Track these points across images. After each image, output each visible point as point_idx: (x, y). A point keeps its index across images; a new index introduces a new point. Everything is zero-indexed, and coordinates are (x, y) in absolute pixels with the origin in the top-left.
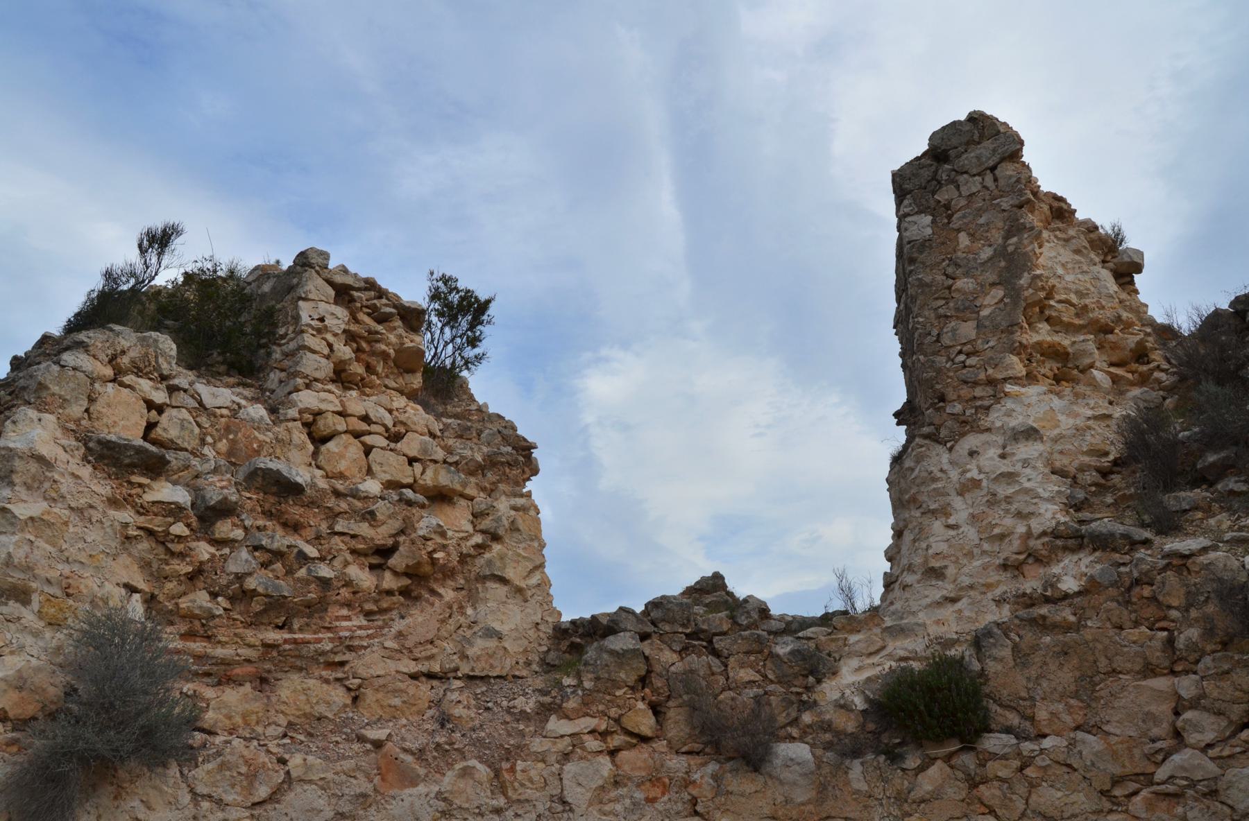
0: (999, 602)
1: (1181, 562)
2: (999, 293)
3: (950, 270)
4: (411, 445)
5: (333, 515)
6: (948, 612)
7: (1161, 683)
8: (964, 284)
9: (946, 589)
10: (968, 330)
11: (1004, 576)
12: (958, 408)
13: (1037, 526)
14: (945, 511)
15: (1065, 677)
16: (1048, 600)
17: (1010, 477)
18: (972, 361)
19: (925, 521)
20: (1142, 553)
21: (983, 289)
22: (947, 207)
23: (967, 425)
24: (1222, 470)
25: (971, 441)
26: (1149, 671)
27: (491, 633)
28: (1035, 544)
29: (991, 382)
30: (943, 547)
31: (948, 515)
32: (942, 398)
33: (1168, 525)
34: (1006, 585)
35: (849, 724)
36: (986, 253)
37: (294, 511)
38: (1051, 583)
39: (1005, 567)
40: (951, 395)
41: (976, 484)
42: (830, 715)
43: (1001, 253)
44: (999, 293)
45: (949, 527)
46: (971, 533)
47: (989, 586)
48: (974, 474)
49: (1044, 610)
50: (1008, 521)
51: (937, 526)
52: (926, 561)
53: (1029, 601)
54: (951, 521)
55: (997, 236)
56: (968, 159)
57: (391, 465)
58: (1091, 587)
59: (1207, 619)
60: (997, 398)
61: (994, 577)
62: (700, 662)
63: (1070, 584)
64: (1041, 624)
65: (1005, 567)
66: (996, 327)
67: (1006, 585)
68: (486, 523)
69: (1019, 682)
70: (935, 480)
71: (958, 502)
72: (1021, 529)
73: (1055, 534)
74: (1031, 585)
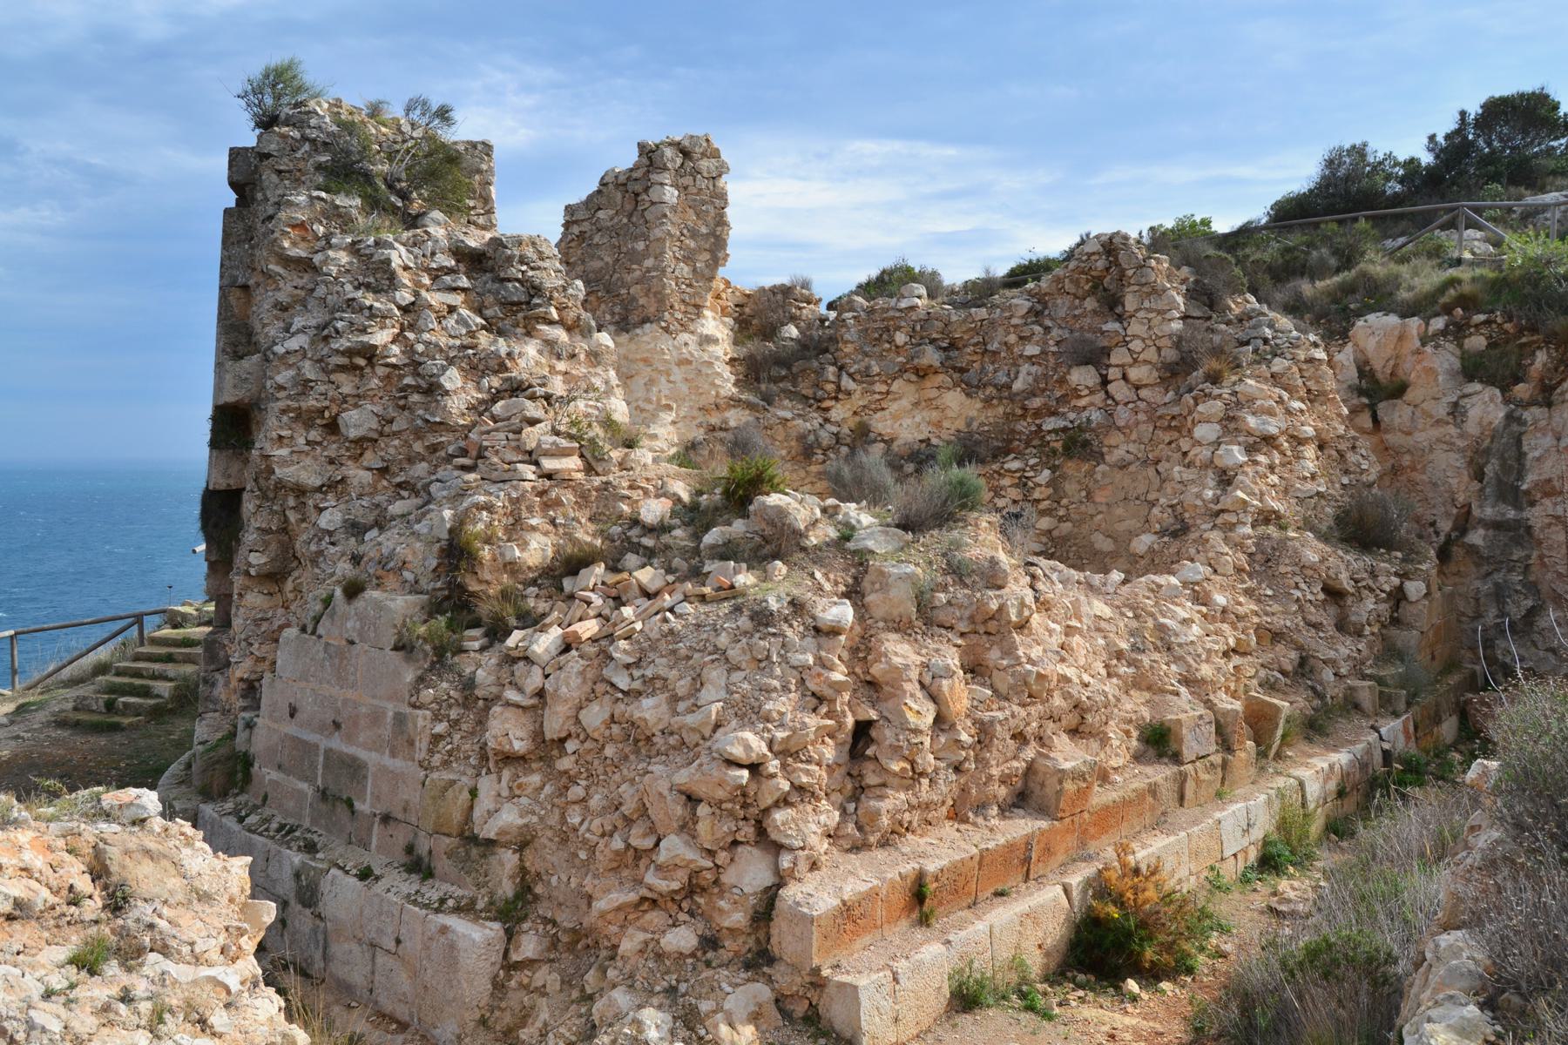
0: (700, 425)
2: (707, 256)
3: (685, 231)
11: (701, 413)
13: (723, 393)
16: (721, 429)
17: (710, 364)
18: (688, 290)
19: (654, 375)
21: (700, 250)
22: (686, 188)
24: (782, 379)
25: (685, 337)
28: (722, 402)
29: (697, 307)
30: (667, 392)
31: (669, 375)
32: (672, 307)
33: (768, 399)
36: (704, 230)
38: (725, 421)
39: (700, 409)
40: (677, 307)
41: (690, 363)
43: (713, 234)
45: (669, 381)
46: (684, 388)
47: (694, 418)
48: (688, 356)
50: (706, 386)
52: (659, 400)
53: (713, 429)
54: (672, 378)
56: (704, 164)
59: (791, 447)
60: (699, 315)
61: (695, 413)
63: (732, 424)
65: (700, 409)
66: (703, 276)
70: (664, 354)
71: (675, 369)
72: (713, 393)
73: (731, 399)
74: (714, 420)
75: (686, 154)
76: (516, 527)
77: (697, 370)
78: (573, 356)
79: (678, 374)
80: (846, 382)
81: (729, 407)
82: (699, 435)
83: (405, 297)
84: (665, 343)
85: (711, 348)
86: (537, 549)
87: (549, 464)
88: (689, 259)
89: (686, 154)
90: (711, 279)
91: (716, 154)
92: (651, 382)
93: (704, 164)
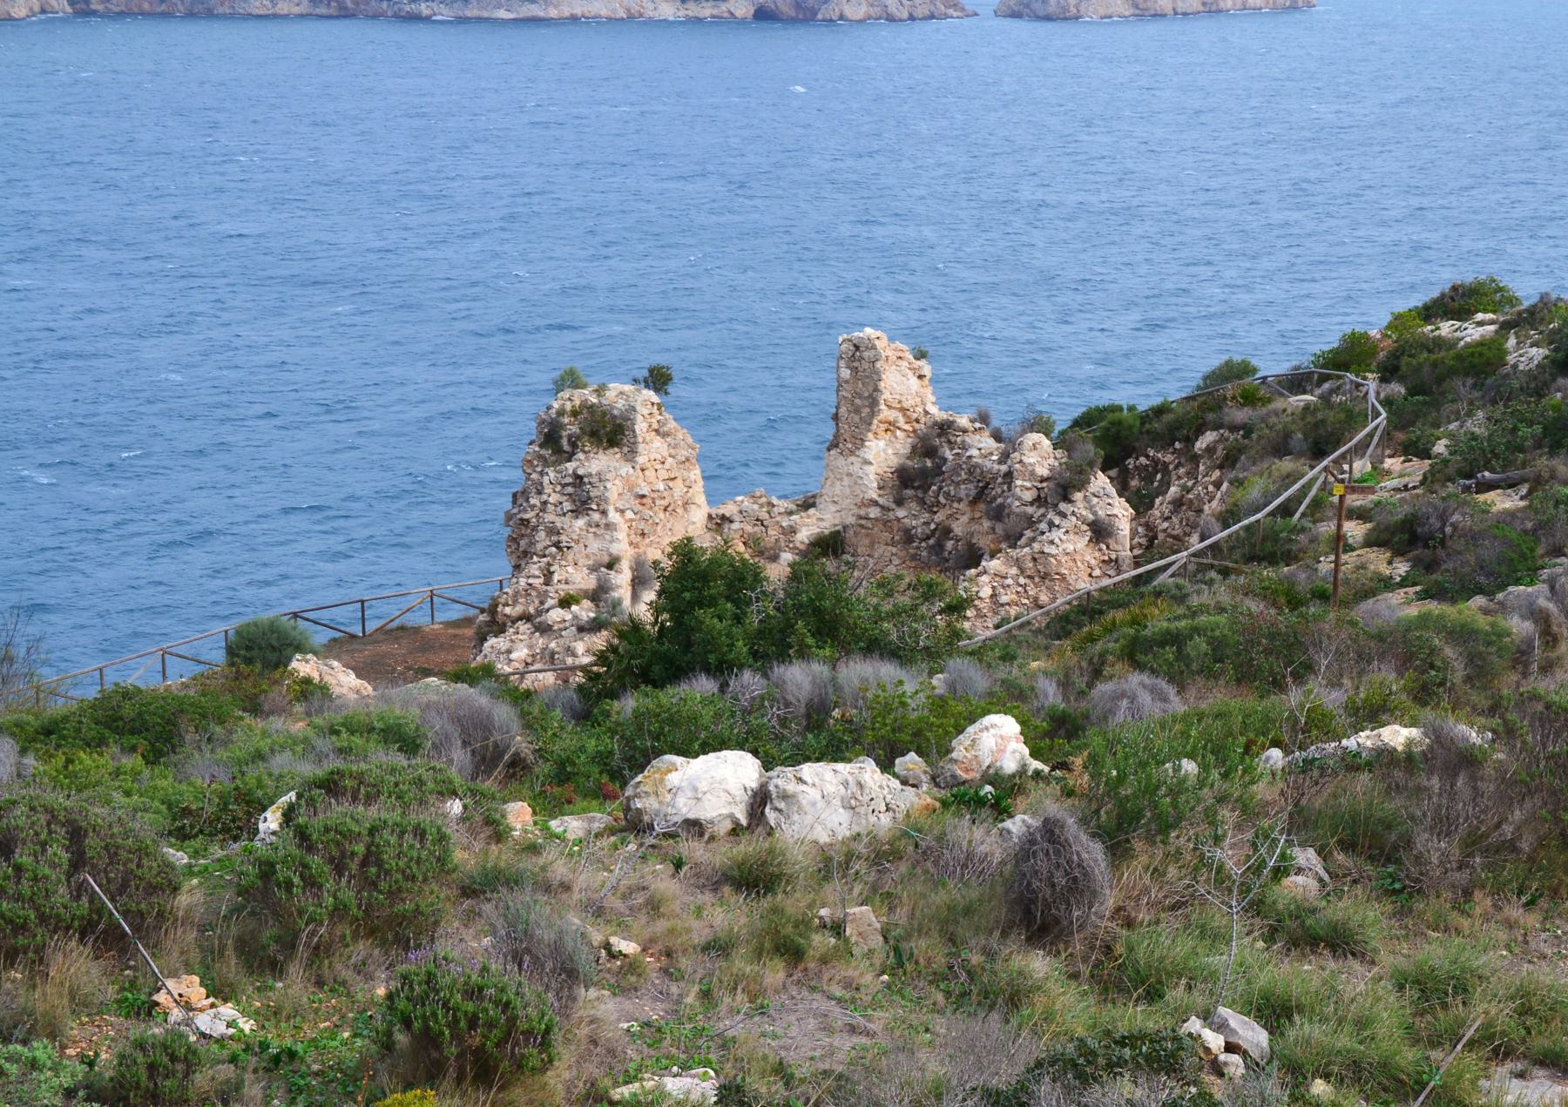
1: (898, 520)
2: (868, 410)
4: (667, 466)
5: (653, 499)
6: (838, 514)
7: (890, 548)
8: (858, 401)
9: (838, 508)
10: (857, 418)
12: (850, 446)
14: (841, 480)
15: (867, 541)
20: (891, 513)
23: (852, 453)
25: (852, 459)
26: (887, 544)
27: (694, 523)
33: (900, 502)
34: (856, 511)
35: (802, 547)
36: (866, 394)
37: (645, 501)
42: (798, 545)
43: (871, 396)
44: (868, 410)
46: (848, 491)
49: (863, 522)
51: (838, 483)
53: (860, 517)
55: (871, 389)
57: (663, 474)
58: (876, 519)
60: (863, 446)
61: (852, 507)
62: (759, 529)
63: (872, 516)
64: (862, 526)
67: (856, 511)
68: (687, 483)
69: (854, 540)
74: (862, 513)
75: (857, 347)
76: (515, 602)
77: (857, 481)
78: (598, 526)
79: (846, 481)
80: (942, 500)
81: (869, 506)
82: (851, 520)
83: (545, 497)
84: (841, 462)
85: (866, 468)
86: (519, 609)
87: (531, 581)
88: (857, 411)
89: (857, 347)
90: (870, 424)
91: (874, 347)
92: (832, 485)
93: (866, 354)
